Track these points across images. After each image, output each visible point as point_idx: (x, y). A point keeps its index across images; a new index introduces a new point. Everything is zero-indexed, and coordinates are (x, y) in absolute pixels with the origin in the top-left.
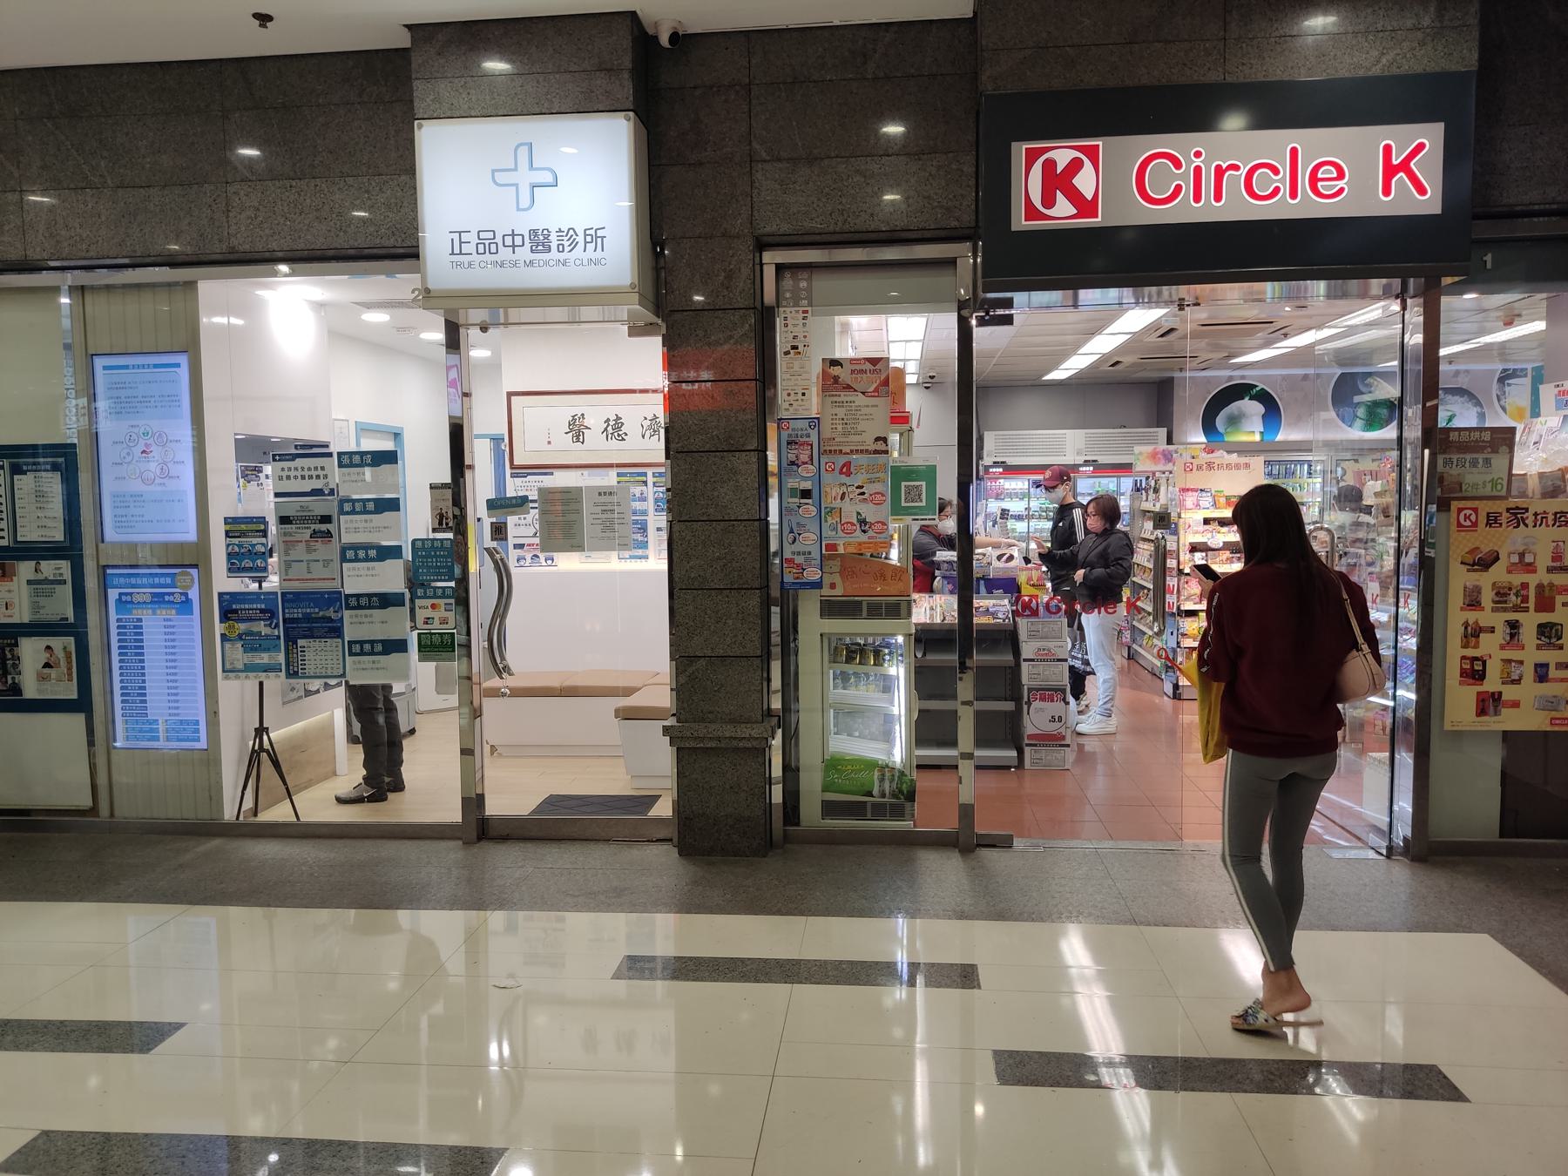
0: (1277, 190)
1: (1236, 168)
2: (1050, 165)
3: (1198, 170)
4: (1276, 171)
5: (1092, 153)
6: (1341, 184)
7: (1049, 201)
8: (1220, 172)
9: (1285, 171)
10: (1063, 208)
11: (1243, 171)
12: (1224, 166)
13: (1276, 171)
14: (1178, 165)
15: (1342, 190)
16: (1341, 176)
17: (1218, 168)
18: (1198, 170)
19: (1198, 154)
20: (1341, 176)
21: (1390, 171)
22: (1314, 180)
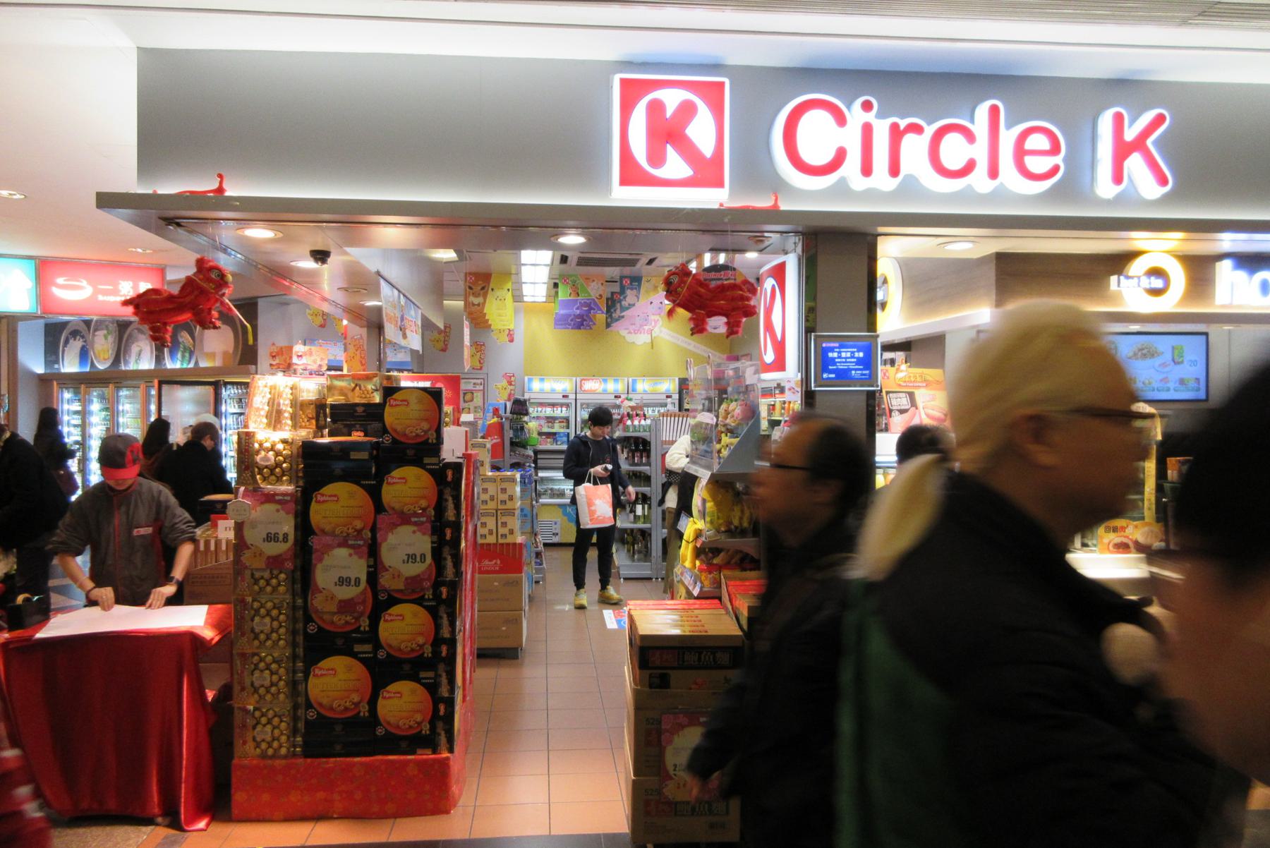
1: (917, 129)
2: (656, 108)
3: (867, 130)
4: (970, 136)
5: (713, 94)
6: (1058, 160)
8: (896, 134)
12: (903, 123)
13: (970, 136)
15: (1055, 169)
16: (1055, 149)
17: (894, 127)
18: (867, 130)
20: (1055, 149)
22: (1020, 153)
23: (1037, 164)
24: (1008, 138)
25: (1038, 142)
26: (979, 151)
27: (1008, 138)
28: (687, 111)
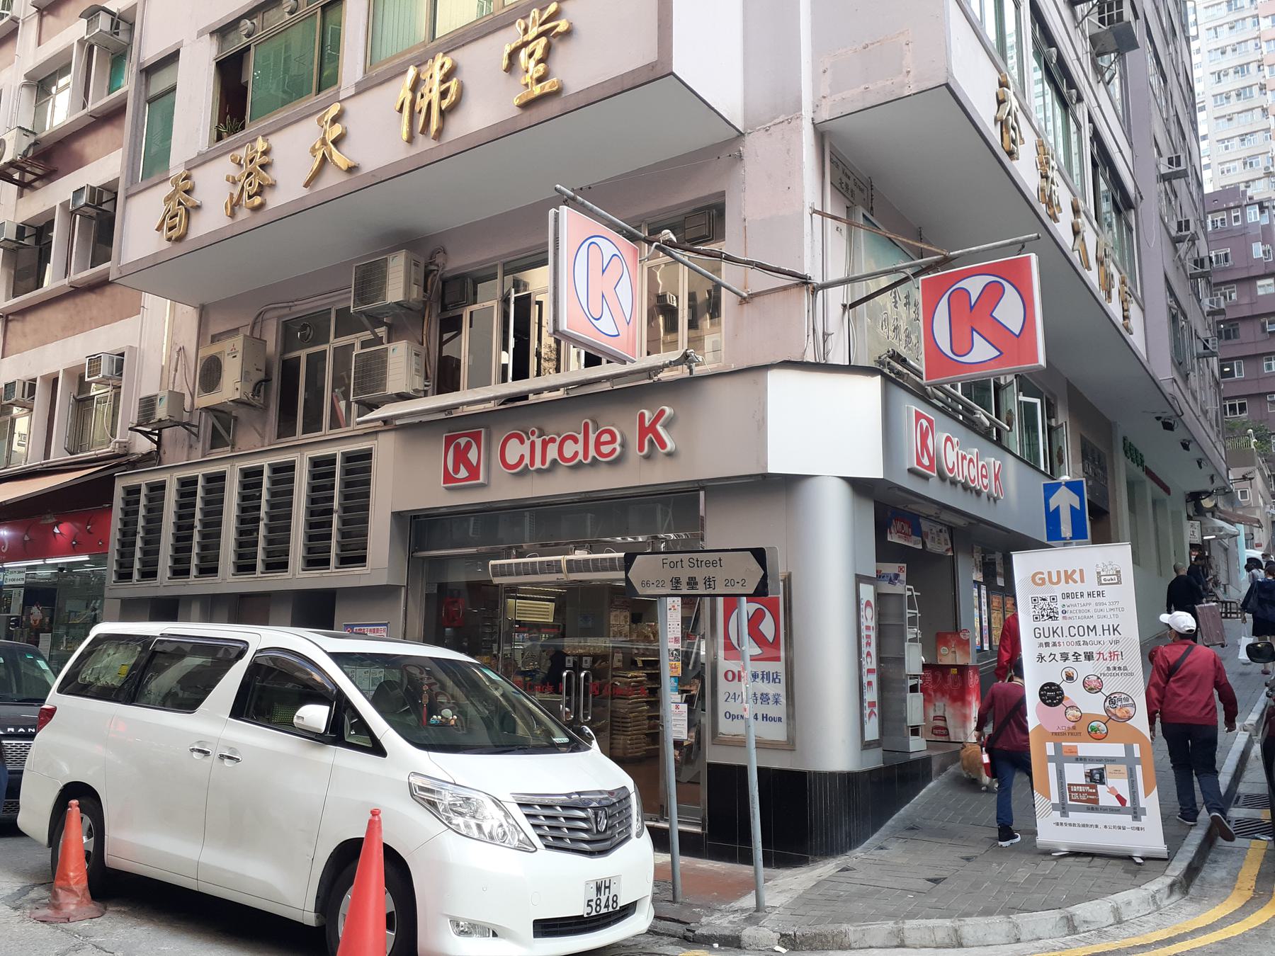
0: (576, 454)
1: (553, 440)
2: (458, 445)
3: (533, 444)
5: (476, 437)
7: (456, 470)
9: (581, 437)
10: (463, 473)
11: (558, 440)
12: (547, 438)
13: (576, 441)
14: (522, 442)
15: (614, 450)
17: (544, 440)
18: (533, 444)
19: (533, 433)
21: (643, 431)
22: (598, 444)
23: (605, 449)
24: (592, 438)
25: (606, 437)
26: (580, 447)
27: (592, 438)
28: (468, 446)
